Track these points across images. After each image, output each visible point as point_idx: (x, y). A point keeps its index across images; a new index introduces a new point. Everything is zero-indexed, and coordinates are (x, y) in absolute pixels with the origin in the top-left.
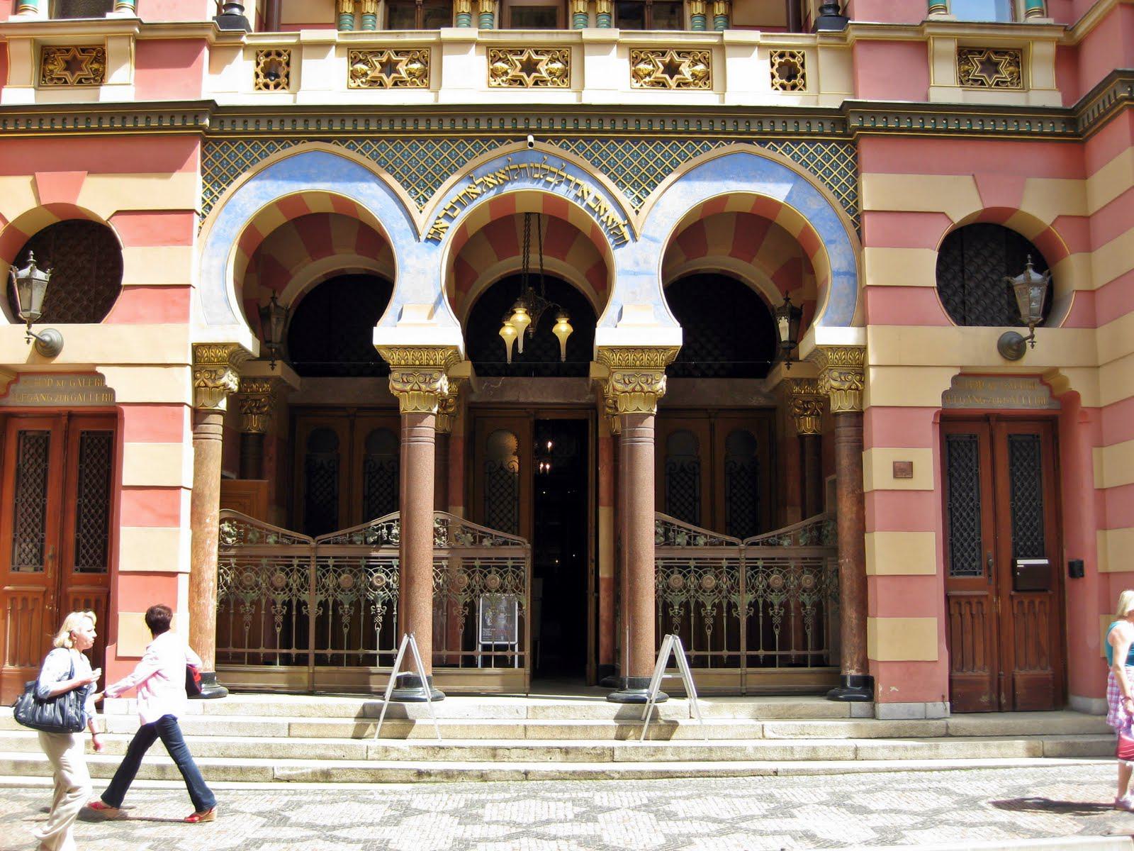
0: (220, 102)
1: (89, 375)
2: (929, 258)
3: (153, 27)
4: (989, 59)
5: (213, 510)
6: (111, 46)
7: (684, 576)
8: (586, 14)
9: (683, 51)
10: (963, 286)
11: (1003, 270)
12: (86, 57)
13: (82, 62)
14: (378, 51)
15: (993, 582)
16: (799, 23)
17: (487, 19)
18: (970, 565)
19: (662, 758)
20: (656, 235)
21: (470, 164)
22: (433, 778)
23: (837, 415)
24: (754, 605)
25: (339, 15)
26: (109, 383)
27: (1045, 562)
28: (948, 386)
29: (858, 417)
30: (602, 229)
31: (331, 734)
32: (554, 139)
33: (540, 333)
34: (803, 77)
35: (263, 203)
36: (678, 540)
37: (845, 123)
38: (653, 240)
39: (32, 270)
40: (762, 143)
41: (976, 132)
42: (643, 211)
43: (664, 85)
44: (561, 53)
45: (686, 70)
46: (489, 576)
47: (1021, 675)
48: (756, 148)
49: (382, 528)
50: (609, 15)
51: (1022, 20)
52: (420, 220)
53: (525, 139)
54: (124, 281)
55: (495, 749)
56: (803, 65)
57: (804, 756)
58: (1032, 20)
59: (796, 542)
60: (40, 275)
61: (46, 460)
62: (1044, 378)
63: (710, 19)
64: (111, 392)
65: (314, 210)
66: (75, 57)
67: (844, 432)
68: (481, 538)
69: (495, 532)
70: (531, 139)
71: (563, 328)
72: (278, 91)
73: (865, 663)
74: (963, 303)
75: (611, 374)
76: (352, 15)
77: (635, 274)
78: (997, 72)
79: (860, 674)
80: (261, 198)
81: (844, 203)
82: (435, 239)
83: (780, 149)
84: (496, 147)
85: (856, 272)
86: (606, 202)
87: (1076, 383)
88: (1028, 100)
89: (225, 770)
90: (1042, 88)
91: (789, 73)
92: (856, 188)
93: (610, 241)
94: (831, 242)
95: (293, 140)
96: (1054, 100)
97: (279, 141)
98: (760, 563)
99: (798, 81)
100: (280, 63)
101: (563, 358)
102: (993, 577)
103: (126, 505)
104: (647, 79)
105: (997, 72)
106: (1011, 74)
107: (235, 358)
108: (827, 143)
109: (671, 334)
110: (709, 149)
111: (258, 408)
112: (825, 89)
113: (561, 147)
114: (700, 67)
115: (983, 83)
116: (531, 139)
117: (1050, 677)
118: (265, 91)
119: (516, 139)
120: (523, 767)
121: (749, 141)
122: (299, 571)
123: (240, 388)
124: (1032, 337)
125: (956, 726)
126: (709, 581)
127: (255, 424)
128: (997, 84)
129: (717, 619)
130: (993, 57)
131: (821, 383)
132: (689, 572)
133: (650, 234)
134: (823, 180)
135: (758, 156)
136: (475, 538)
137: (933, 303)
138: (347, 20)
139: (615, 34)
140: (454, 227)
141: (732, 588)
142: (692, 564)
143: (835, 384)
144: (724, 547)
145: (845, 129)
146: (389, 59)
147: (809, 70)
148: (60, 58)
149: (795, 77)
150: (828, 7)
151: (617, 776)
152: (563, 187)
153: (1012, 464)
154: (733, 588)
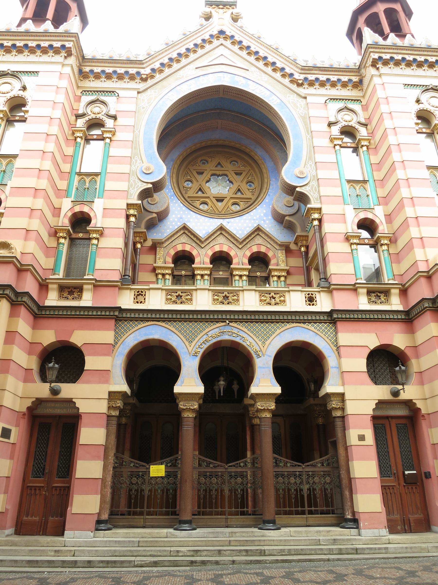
0: (123, 307)
1: (70, 402)
2: (364, 361)
4: (377, 295)
5: (112, 453)
6: (85, 287)
7: (283, 478)
10: (374, 371)
11: (387, 365)
12: (76, 290)
13: (74, 292)
15: (397, 480)
16: (310, 284)
18: (387, 473)
19: (283, 554)
20: (270, 355)
21: (207, 330)
22: (197, 564)
23: (335, 417)
24: (309, 489)
25: (157, 279)
26: (77, 405)
27: (415, 472)
28: (374, 407)
29: (343, 418)
30: (252, 352)
31: (154, 545)
32: (235, 322)
33: (228, 388)
34: (316, 301)
35: (136, 342)
36: (281, 464)
37: (331, 316)
38: (270, 356)
39: (54, 364)
40: (304, 323)
41: (376, 319)
42: (266, 347)
43: (270, 304)
44: (236, 293)
45: (278, 300)
46: (213, 479)
47: (412, 517)
48: (302, 325)
49: (173, 460)
50: (246, 281)
51: (386, 282)
52: (190, 349)
53: (225, 322)
54: (85, 369)
55: (219, 551)
56: (315, 297)
57: (337, 552)
58: (391, 282)
59: (323, 465)
60: (56, 366)
61: (49, 434)
62: (409, 403)
63: (279, 282)
64: (78, 409)
65: (152, 345)
66: (72, 290)
67: (339, 423)
68: (209, 464)
69: (215, 462)
70: (227, 322)
71: (236, 387)
72: (142, 304)
73: (354, 513)
74: (375, 377)
75: (256, 402)
76: (161, 279)
77: (264, 368)
78: (380, 299)
79: (352, 518)
80: (135, 340)
81: (333, 343)
82: (195, 355)
83: (310, 325)
84: (216, 324)
85: (339, 366)
86: (254, 343)
87: (419, 404)
88: (391, 307)
89: (115, 562)
90: (395, 304)
91: (311, 300)
92: (336, 338)
93: (254, 356)
94: (329, 356)
95: (147, 321)
96: (401, 308)
97: (142, 321)
98: (310, 473)
99: (314, 303)
100: (142, 295)
101: (236, 397)
102: (397, 478)
103: (79, 452)
104: (265, 302)
105: (380, 299)
106: (385, 299)
108: (325, 323)
109: (277, 389)
110: (286, 325)
111: (126, 414)
113: (237, 324)
114: (282, 298)
115: (376, 303)
116: (227, 322)
117: (423, 518)
118: (137, 304)
119: (222, 322)
120: (231, 558)
122: (142, 477)
123: (123, 407)
124: (404, 389)
125: (392, 539)
126: (292, 480)
127: (124, 420)
128: (381, 303)
129: (296, 495)
130: (379, 294)
131: (328, 406)
132: (285, 477)
133: (268, 354)
134: (325, 335)
135: (302, 327)
136: (207, 464)
137: (366, 376)
138: (160, 281)
139: (254, 287)
140: (202, 351)
141: (301, 483)
142: (286, 473)
143: (334, 406)
144: (297, 467)
145: (331, 318)
146: (179, 295)
147: (318, 299)
148: (67, 290)
149: (313, 302)
150: (323, 278)
151: (268, 562)
152: (239, 338)
153: (398, 435)
154: (301, 483)
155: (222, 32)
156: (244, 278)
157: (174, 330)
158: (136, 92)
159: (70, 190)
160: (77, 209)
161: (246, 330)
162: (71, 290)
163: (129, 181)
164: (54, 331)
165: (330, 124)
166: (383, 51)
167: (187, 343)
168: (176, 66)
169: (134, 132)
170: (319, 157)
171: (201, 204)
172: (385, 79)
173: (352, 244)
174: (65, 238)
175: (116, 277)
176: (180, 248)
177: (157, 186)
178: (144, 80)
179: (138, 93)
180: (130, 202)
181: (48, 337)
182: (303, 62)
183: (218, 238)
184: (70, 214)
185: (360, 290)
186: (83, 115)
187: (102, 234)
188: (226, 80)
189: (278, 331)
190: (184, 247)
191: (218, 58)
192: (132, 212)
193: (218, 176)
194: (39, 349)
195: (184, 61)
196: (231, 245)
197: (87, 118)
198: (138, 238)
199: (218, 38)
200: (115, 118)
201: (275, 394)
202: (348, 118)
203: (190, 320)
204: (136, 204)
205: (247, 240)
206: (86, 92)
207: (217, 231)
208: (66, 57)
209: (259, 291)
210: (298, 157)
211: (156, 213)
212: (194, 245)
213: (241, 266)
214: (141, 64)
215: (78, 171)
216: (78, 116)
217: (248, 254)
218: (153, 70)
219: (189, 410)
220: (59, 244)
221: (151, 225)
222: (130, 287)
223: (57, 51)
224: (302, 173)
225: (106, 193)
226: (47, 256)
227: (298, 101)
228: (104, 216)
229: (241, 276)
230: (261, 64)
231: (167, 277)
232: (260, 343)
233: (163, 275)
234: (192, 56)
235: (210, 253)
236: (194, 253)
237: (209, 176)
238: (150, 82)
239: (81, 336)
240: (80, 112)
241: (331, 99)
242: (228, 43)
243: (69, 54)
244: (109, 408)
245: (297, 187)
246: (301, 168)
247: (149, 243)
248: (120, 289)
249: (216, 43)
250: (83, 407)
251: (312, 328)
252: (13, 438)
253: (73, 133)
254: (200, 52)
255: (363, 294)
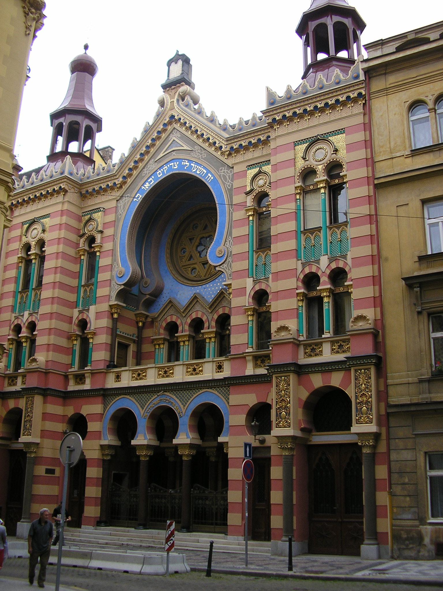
3: (93, 370)
6: (86, 375)
8: (209, 342)
9: (197, 364)
14: (136, 370)
17: (187, 347)
40: (211, 388)
45: (197, 371)
48: (210, 390)
64: (85, 456)
91: (220, 367)
99: (222, 370)
107: (110, 446)
112: (226, 373)
121: (208, 388)
140: (149, 414)
152: (170, 403)
155: (172, 117)
156: (213, 340)
157: (134, 400)
158: (116, 201)
159: (78, 301)
160: (80, 318)
161: (174, 397)
162: (80, 378)
163: (110, 286)
164: (72, 407)
165: (247, 193)
166: (275, 112)
167: (141, 409)
168: (141, 165)
169: (114, 239)
170: (236, 232)
171: (192, 270)
172: (280, 142)
173: (248, 315)
174: (76, 340)
175: (102, 366)
176: (169, 320)
177: (129, 284)
178: (121, 187)
179: (117, 201)
180: (112, 303)
181: (70, 411)
182: (231, 129)
183: (196, 306)
184: (77, 322)
185: (247, 358)
186: (84, 234)
187: (95, 334)
188: (175, 167)
189: (195, 396)
190: (171, 318)
191: (172, 145)
192: (113, 311)
193: (207, 238)
194: (67, 419)
195: (146, 158)
196: (204, 311)
197: (85, 237)
198: (138, 318)
199: (170, 123)
200: (101, 232)
201: (187, 444)
202: (261, 182)
203: (143, 393)
204: (115, 304)
205: (216, 304)
206: (85, 214)
207: (193, 300)
208: (64, 195)
209: (187, 365)
210: (221, 234)
211: (149, 294)
212: (179, 315)
213: (210, 330)
214: (113, 176)
215: (83, 283)
216: (81, 236)
217: (216, 317)
218: (124, 177)
219: (143, 455)
220: (73, 345)
221: (149, 304)
222: (112, 371)
223: (58, 192)
224: (221, 251)
225: (98, 300)
226: (68, 354)
227: (227, 172)
228: (97, 318)
229: (210, 338)
230: (200, 141)
231: (162, 346)
232: (182, 406)
233: (159, 345)
234: (152, 150)
235: (189, 321)
236: (178, 323)
237: (198, 241)
238: (125, 188)
239: (86, 410)
240: (81, 233)
241: (249, 166)
242: (177, 126)
243: (66, 191)
244: (103, 455)
245: (217, 266)
246: (221, 247)
247: (149, 320)
248: (106, 373)
249: (169, 128)
250: (88, 455)
251: (216, 393)
252: (57, 473)
253: (79, 253)
254: (158, 143)
255: (249, 361)
